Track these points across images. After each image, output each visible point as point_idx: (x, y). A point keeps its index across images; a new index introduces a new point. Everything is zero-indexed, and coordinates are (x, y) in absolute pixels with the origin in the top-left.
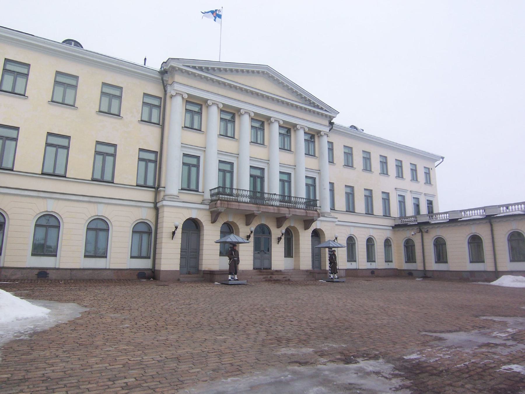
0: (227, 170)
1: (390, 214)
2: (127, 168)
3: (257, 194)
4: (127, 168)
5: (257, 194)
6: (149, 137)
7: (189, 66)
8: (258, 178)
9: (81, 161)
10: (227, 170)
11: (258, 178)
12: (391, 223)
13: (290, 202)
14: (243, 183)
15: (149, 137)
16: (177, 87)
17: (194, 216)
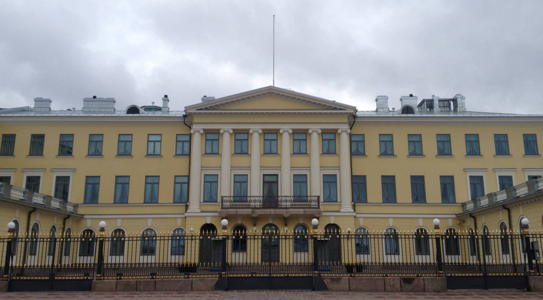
0: (241, 182)
1: (455, 200)
2: (166, 192)
3: (271, 197)
4: (166, 192)
5: (271, 197)
6: (179, 166)
7: (202, 109)
8: (271, 183)
9: (137, 192)
10: (241, 182)
11: (271, 183)
12: (458, 210)
13: (307, 201)
14: (256, 190)
15: (179, 166)
16: (195, 127)
17: (209, 222)
